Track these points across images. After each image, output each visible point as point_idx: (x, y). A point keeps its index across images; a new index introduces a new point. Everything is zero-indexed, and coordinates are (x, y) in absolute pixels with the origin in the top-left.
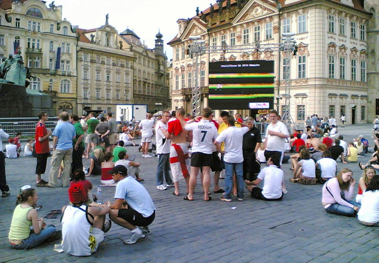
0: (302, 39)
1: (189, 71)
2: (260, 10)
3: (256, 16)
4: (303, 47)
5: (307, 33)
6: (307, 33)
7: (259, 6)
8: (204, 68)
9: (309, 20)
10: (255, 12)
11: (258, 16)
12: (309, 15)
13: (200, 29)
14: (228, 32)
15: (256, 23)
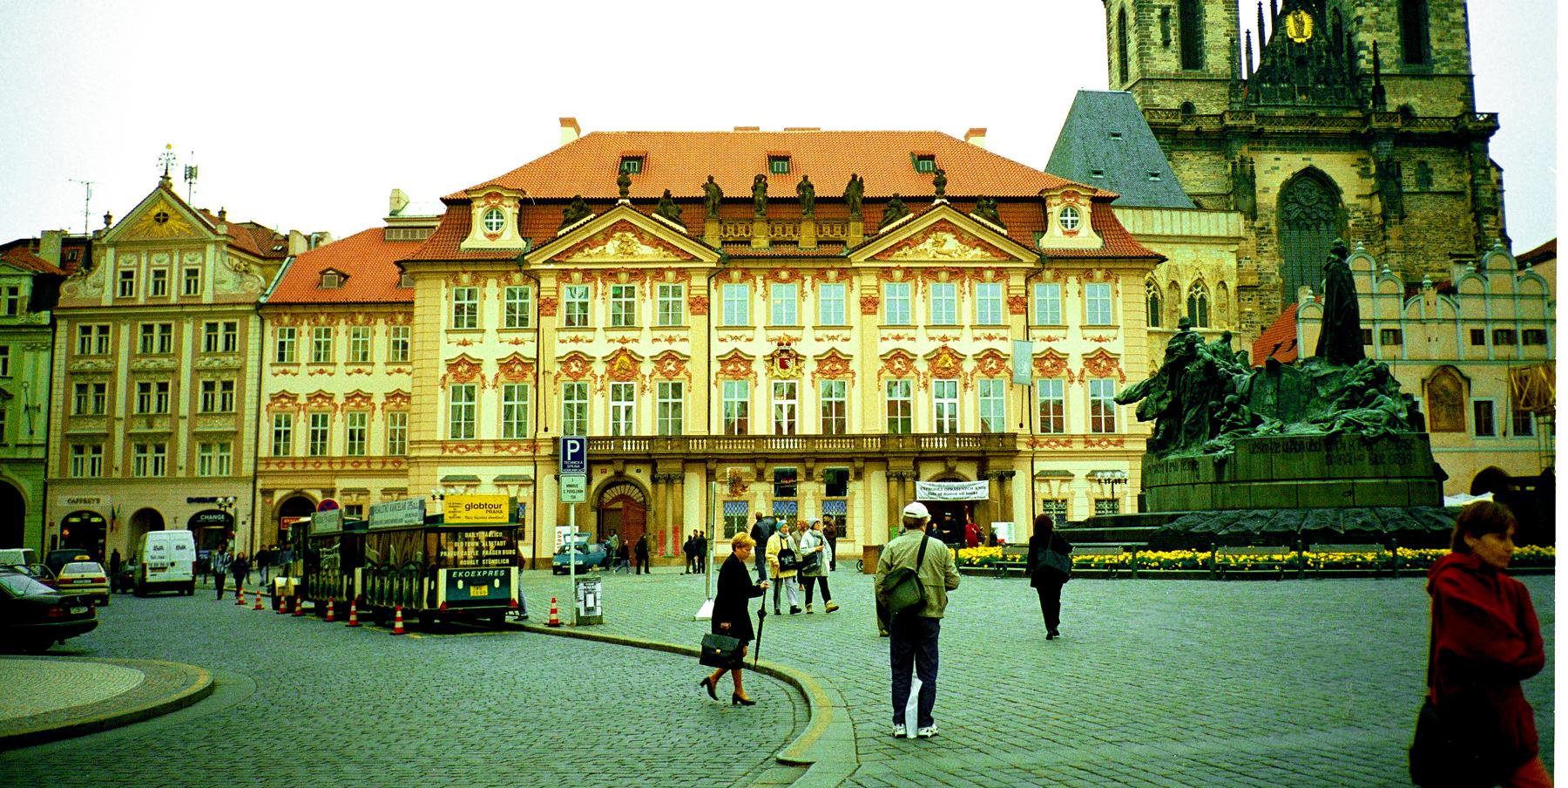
0: (1100, 340)
1: (576, 376)
2: (951, 243)
3: (940, 257)
4: (1107, 359)
5: (1117, 327)
6: (1117, 327)
7: (952, 231)
8: (682, 374)
9: (1119, 300)
10: (936, 243)
11: (947, 258)
12: (1119, 287)
13: (658, 242)
14: (809, 279)
15: (944, 275)
